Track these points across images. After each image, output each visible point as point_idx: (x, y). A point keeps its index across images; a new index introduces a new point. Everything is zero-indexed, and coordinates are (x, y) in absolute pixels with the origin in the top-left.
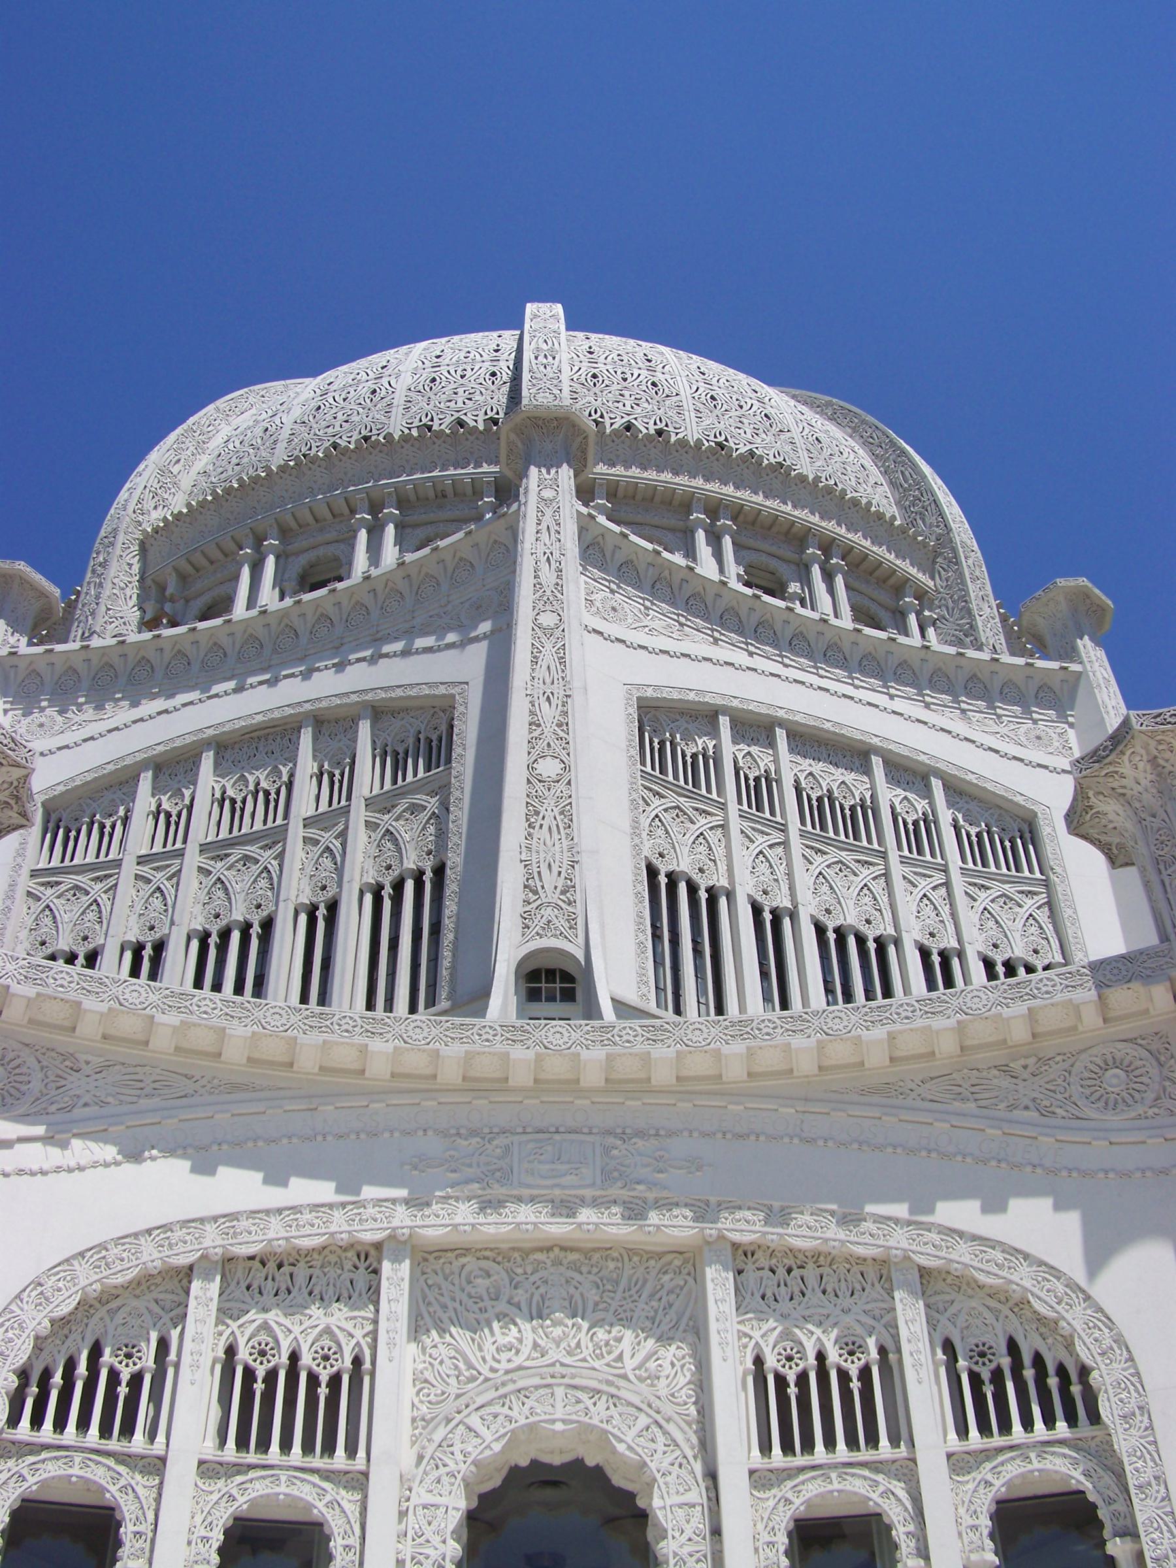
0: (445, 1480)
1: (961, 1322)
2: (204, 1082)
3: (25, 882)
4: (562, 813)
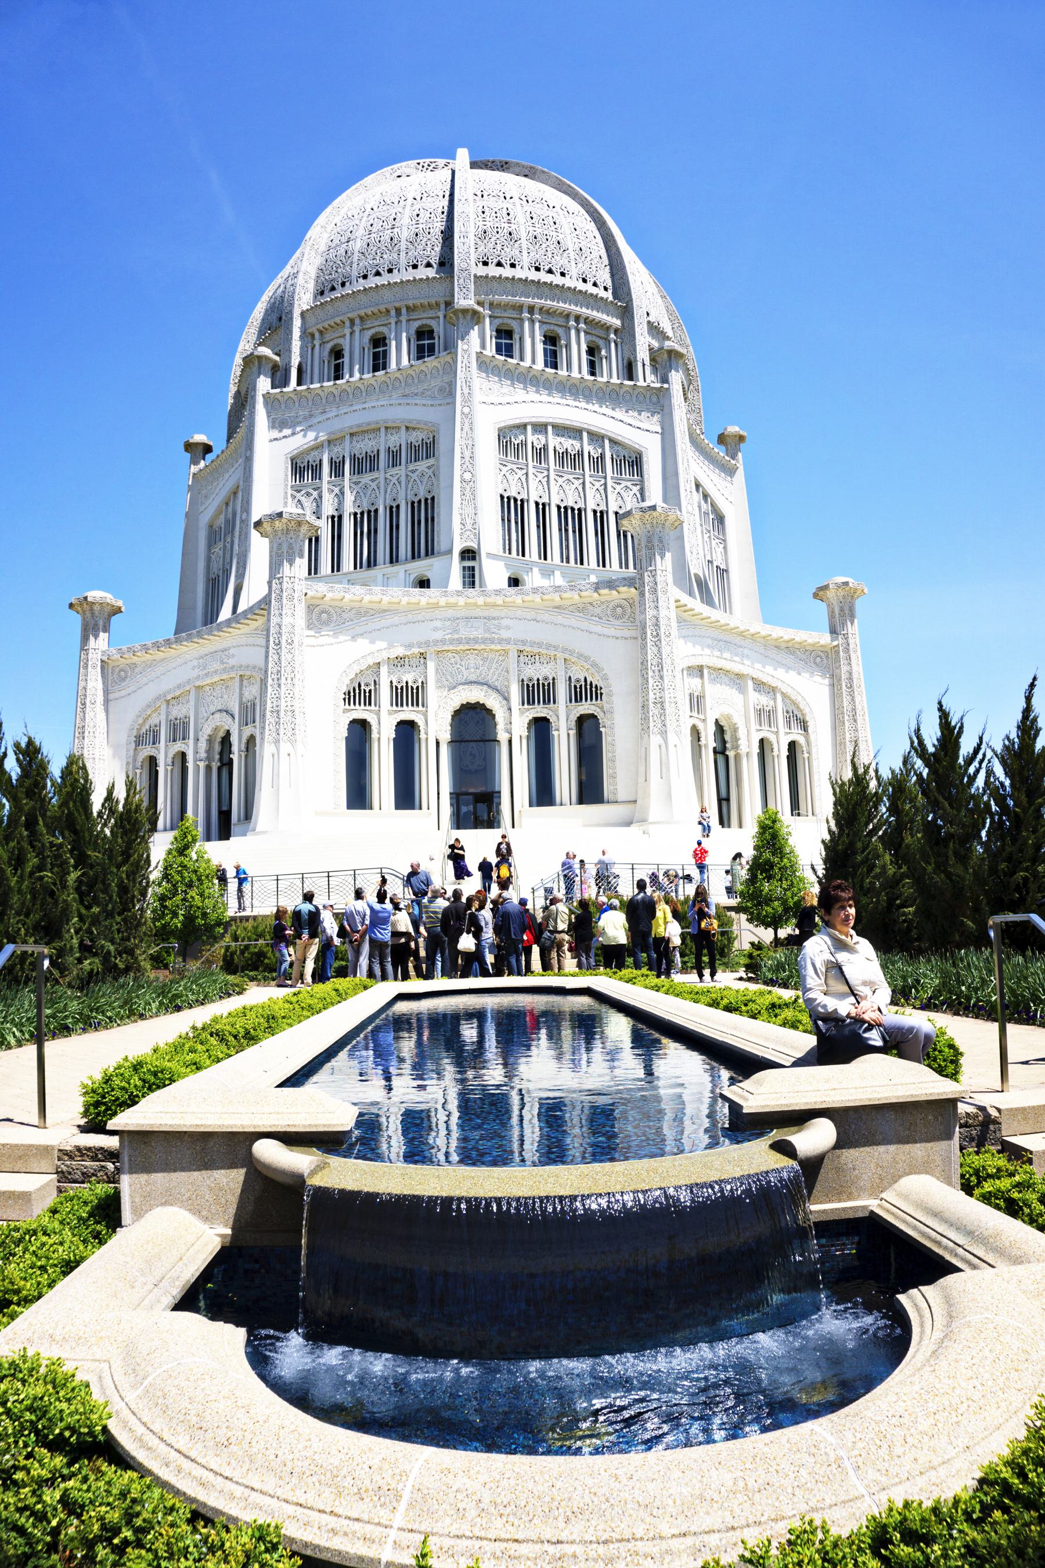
3: (290, 491)
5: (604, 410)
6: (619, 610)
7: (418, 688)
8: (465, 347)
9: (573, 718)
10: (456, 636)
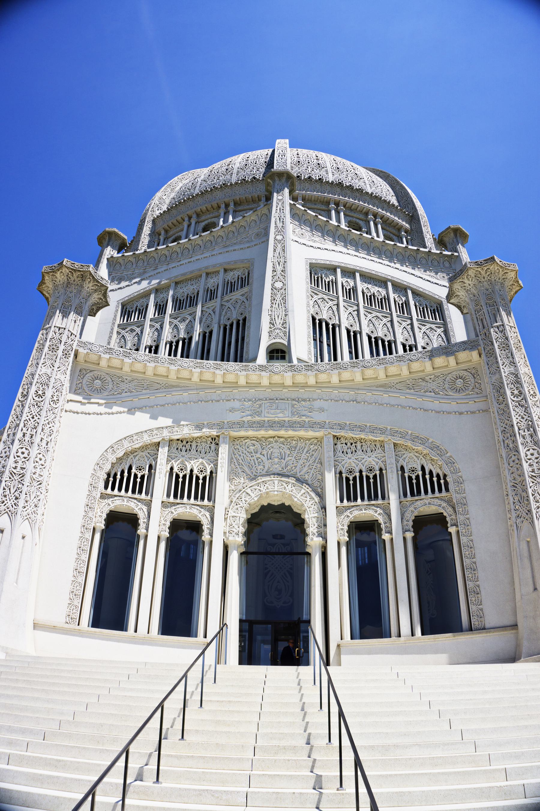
0: (239, 509)
1: (406, 460)
2: (162, 385)
4: (282, 299)
5: (404, 268)
6: (459, 382)
7: (204, 478)
8: (280, 198)
9: (410, 517)
10: (257, 419)
